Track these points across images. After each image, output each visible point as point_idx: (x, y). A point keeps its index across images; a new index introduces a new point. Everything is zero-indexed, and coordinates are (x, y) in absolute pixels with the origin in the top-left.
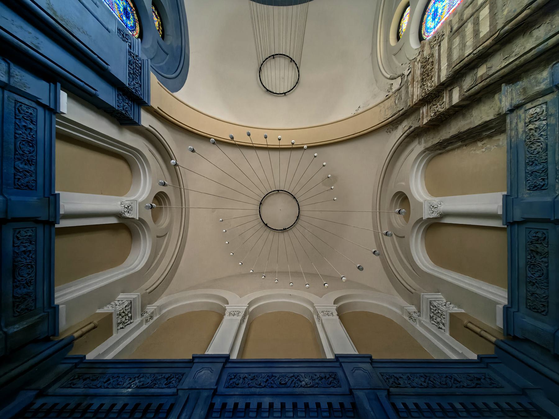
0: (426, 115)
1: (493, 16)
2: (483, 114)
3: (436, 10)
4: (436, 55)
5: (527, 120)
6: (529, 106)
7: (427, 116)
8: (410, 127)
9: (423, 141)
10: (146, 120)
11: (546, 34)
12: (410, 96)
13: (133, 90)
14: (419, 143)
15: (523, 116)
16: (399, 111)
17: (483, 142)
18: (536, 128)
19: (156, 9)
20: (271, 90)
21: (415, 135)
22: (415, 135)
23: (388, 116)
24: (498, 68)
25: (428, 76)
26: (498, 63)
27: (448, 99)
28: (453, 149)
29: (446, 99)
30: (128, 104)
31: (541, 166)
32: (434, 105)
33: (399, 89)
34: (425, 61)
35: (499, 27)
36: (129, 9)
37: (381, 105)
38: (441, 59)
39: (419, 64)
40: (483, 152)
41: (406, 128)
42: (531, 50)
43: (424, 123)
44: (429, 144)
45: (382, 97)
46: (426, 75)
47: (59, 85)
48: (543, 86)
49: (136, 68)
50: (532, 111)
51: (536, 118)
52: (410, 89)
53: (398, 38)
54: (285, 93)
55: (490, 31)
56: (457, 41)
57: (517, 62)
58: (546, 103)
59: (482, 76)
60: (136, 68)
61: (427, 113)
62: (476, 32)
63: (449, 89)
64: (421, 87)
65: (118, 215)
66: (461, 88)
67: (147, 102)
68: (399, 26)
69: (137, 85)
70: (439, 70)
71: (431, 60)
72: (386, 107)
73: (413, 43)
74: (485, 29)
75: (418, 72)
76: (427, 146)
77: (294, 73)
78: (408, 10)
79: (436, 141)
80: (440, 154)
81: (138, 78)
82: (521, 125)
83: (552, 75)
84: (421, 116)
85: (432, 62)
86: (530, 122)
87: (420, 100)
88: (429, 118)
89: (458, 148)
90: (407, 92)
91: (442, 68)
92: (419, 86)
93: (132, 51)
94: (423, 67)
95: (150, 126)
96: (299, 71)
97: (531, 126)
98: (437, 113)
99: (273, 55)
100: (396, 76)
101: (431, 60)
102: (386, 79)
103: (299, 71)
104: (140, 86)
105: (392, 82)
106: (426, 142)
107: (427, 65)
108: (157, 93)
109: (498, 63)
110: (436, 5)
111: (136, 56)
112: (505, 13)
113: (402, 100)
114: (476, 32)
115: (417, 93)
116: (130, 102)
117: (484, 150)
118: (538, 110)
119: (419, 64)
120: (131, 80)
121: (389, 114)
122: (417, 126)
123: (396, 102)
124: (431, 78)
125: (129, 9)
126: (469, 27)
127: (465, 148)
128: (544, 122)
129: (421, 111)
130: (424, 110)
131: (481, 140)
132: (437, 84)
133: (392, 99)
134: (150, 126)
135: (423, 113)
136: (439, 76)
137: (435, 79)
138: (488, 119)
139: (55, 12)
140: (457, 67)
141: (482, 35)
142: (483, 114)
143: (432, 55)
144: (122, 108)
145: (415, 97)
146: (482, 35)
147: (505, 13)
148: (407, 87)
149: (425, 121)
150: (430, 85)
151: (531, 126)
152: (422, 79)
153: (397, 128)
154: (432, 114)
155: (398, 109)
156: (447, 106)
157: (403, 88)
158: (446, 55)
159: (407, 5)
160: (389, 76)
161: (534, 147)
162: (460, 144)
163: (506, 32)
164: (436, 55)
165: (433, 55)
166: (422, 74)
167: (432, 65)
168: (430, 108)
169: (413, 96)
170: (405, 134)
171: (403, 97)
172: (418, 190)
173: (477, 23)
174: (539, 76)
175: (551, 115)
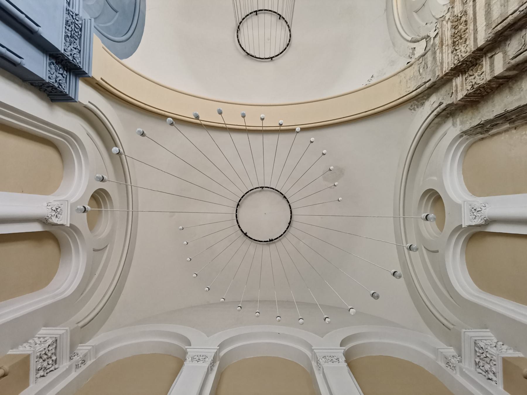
0: (461, 87)
4: (470, 12)
7: (462, 90)
8: (441, 104)
9: (458, 122)
10: (85, 94)
12: (439, 64)
13: (70, 58)
14: (454, 124)
16: (425, 83)
20: (253, 54)
25: (461, 38)
27: (488, 68)
30: (62, 74)
32: (470, 76)
33: (424, 55)
34: (456, 20)
37: (401, 74)
38: (477, 18)
39: (449, 22)
43: (459, 99)
44: (467, 127)
45: (402, 64)
46: (458, 38)
49: (75, 30)
52: (438, 55)
54: (272, 58)
60: (75, 30)
61: (462, 86)
63: (489, 55)
64: (452, 52)
65: (43, 221)
66: (505, 53)
67: (87, 72)
69: (75, 51)
70: (475, 31)
71: (464, 19)
72: (408, 78)
75: (448, 33)
77: (283, 32)
79: (476, 122)
80: (482, 139)
81: (77, 42)
84: (454, 89)
85: (466, 21)
87: (452, 69)
88: (465, 93)
89: (506, 131)
90: (434, 58)
92: (450, 51)
93: (70, 9)
95: (89, 102)
96: (290, 30)
98: (476, 86)
99: (256, 11)
100: (419, 38)
101: (464, 19)
102: (406, 42)
103: (290, 30)
104: (80, 52)
105: (413, 45)
106: (462, 123)
107: (459, 25)
111: (76, 15)
113: (428, 70)
115: (448, 60)
116: (65, 72)
119: (449, 22)
120: (68, 44)
122: (450, 102)
123: (421, 71)
124: (465, 41)
127: (514, 131)
129: (454, 84)
130: (458, 81)
132: (473, 50)
133: (416, 67)
134: (89, 102)
135: (456, 86)
136: (475, 39)
140: (499, 28)
143: (466, 13)
144: (54, 81)
148: (435, 53)
149: (460, 96)
152: (454, 42)
153: (423, 104)
155: (424, 80)
156: (489, 78)
157: (429, 54)
158: (483, 13)
160: (409, 38)
162: (507, 126)
164: (470, 12)
165: (466, 12)
166: (453, 36)
167: (466, 25)
168: (466, 79)
169: (442, 63)
170: (435, 113)
171: (429, 66)
172: (454, 188)
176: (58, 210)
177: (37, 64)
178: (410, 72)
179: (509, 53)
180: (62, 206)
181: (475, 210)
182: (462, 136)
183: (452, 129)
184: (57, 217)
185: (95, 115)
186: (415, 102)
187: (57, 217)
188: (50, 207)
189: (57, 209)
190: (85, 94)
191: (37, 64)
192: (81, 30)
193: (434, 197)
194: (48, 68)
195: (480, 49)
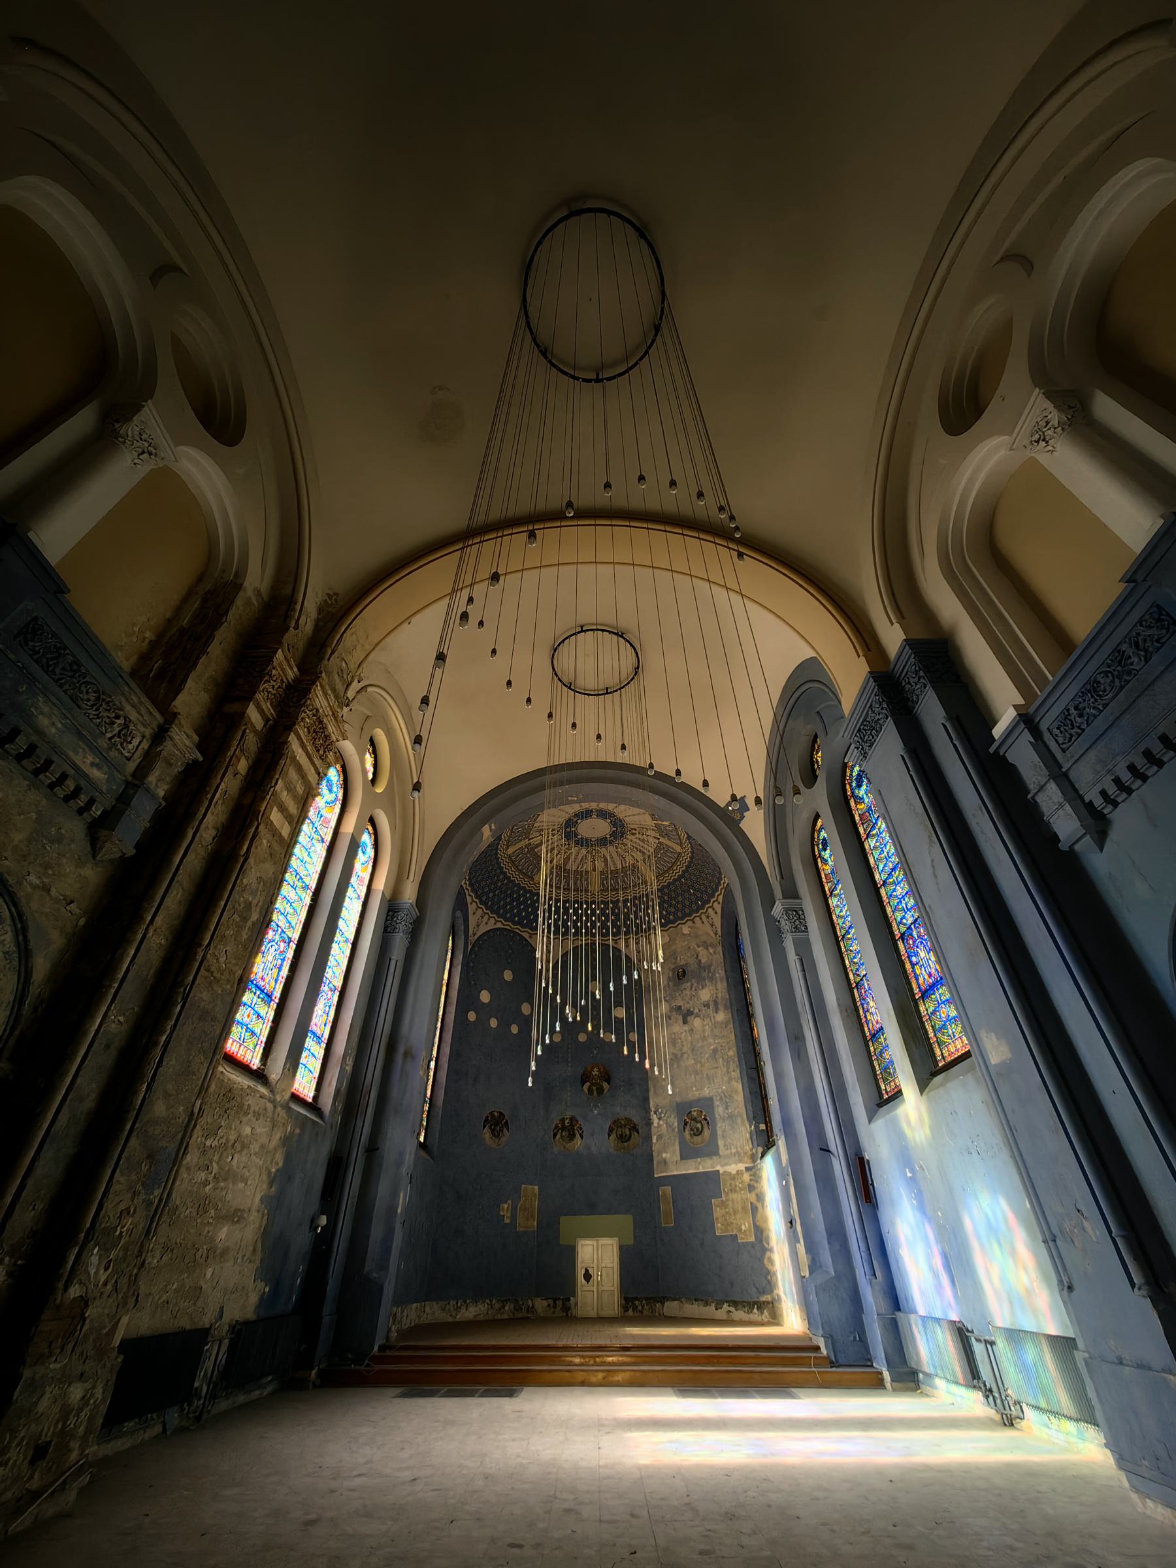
0: (284, 666)
1: (275, 833)
2: (192, 699)
3: (330, 791)
5: (131, 727)
6: (145, 745)
7: (281, 665)
8: (297, 627)
9: (254, 600)
10: (892, 637)
11: (201, 836)
14: (258, 592)
15: (143, 729)
16: (333, 653)
17: (147, 641)
18: (113, 723)
19: (814, 771)
21: (279, 606)
22: (279, 606)
23: (349, 632)
24: (226, 779)
25: (315, 731)
26: (229, 784)
28: (185, 600)
29: (267, 707)
31: (58, 671)
33: (349, 685)
35: (262, 827)
36: (854, 784)
37: (368, 648)
40: (134, 625)
41: (302, 620)
42: (205, 815)
43: (280, 652)
47: (991, 750)
48: (152, 779)
49: (866, 734)
50: (135, 742)
51: (125, 734)
53: (372, 742)
55: (268, 818)
56: (300, 789)
57: (209, 796)
58: (129, 759)
59: (239, 760)
61: (283, 670)
62: (282, 809)
64: (317, 710)
68: (375, 753)
70: (303, 746)
71: (321, 752)
73: (348, 747)
74: (275, 816)
75: (331, 728)
76: (241, 593)
78: (370, 776)
79: (232, 615)
80: (200, 579)
82: (133, 715)
83: (153, 796)
86: (127, 727)
87: (308, 690)
89: (178, 611)
90: (334, 690)
91: (300, 750)
94: (327, 737)
95: (892, 624)
97: (121, 721)
98: (267, 678)
101: (321, 752)
104: (871, 707)
105: (363, 684)
106: (248, 602)
107: (325, 748)
108: (850, 678)
109: (229, 784)
110: (334, 795)
112: (265, 842)
114: (282, 809)
115: (320, 699)
117: (136, 629)
118: (130, 747)
121: (349, 639)
125: (854, 784)
126: (293, 809)
127: (168, 615)
128: (109, 735)
129: (295, 669)
130: (292, 673)
131: (154, 645)
135: (291, 668)
136: (299, 738)
137: (302, 732)
138: (180, 697)
139: (930, 837)
140: (282, 762)
141: (275, 809)
142: (192, 699)
144: (922, 680)
145: (320, 693)
146: (275, 809)
147: (265, 842)
150: (306, 718)
151: (121, 721)
152: (321, 722)
153: (320, 610)
154: (274, 672)
156: (259, 696)
159: (373, 781)
160: (369, 689)
161: (92, 696)
163: (250, 825)
166: (324, 728)
169: (325, 694)
170: (298, 607)
171: (336, 677)
172: (202, 471)
173: (289, 817)
174: (166, 787)
175: (110, 749)
176: (1037, 436)
177: (932, 711)
178: (358, 655)
179: (251, 735)
180: (1026, 442)
181: (150, 454)
182: (237, 575)
183: (257, 579)
184: (1047, 423)
185: (894, 595)
186: (334, 611)
187: (1047, 423)
188: (1050, 448)
189: (1037, 442)
190: (892, 637)
191: (932, 711)
192: (859, 730)
193: (221, 422)
194: (921, 697)
195: (289, 728)
